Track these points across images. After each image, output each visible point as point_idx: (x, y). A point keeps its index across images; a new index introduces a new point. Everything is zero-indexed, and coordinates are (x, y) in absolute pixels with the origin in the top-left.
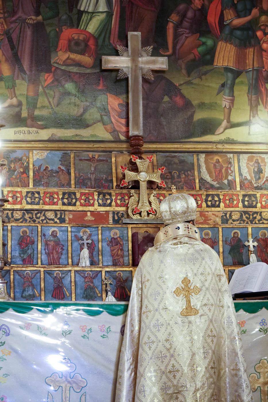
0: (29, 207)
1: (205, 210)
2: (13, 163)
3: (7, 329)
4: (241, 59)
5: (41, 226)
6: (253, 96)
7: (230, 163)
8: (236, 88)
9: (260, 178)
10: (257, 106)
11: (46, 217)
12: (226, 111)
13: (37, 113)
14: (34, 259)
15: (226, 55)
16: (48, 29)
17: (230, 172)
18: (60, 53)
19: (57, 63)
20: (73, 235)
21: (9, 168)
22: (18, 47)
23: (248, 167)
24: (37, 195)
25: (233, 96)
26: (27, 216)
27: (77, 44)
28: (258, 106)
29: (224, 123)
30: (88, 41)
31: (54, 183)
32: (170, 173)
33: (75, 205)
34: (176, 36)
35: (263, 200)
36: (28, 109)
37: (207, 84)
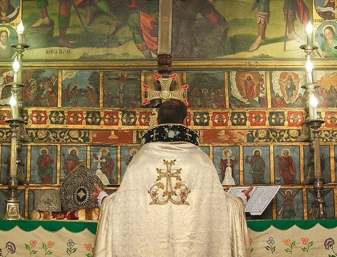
0: (54, 126)
1: (231, 128)
2: (41, 83)
3: (13, 246)
5: (61, 146)
7: (262, 80)
9: (292, 95)
11: (70, 136)
12: (261, 26)
13: (69, 32)
14: (53, 178)
17: (261, 89)
20: (92, 154)
21: (38, 88)
23: (280, 84)
24: (61, 115)
25: (269, 12)
26: (51, 136)
28: (295, 21)
29: (259, 39)
31: (83, 102)
32: (200, 91)
33: (99, 124)
35: (291, 117)
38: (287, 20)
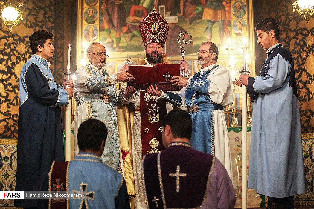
4: (215, 16)
6: (221, 33)
8: (213, 29)
10: (223, 37)
13: (120, 45)
15: (208, 14)
16: (125, 7)
18: (131, 17)
19: (130, 22)
22: (112, 15)
25: (212, 33)
27: (139, 13)
30: (143, 11)
34: (185, 7)
36: (117, 43)
37: (199, 29)
38: (220, 37)
